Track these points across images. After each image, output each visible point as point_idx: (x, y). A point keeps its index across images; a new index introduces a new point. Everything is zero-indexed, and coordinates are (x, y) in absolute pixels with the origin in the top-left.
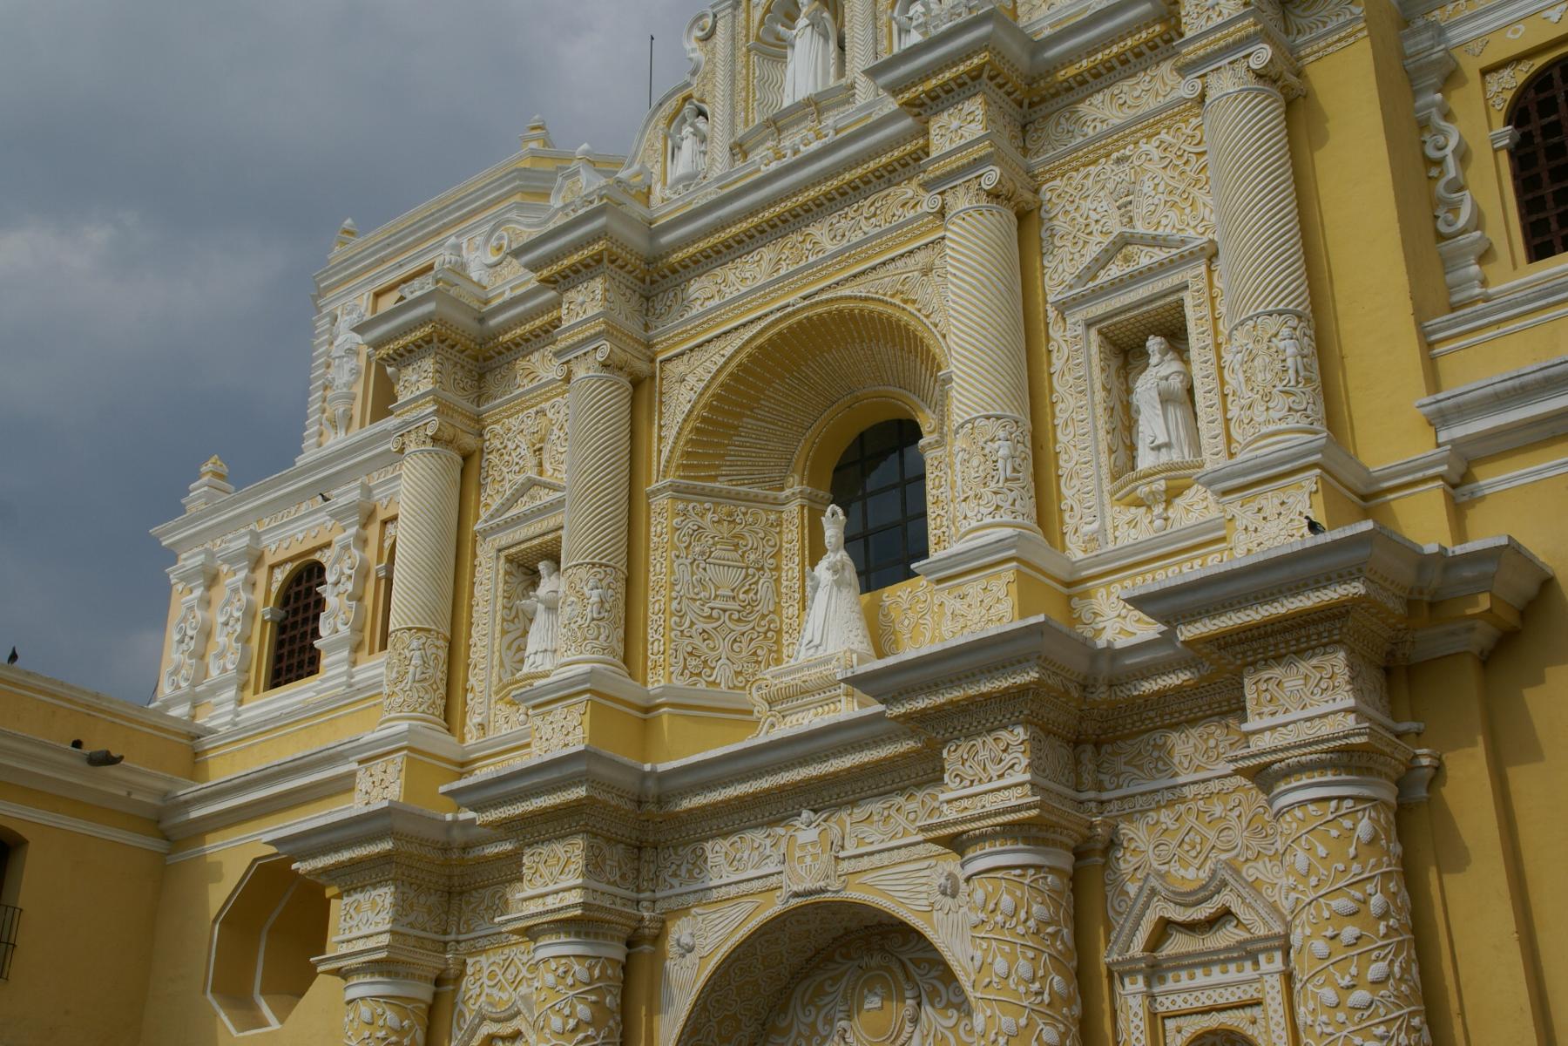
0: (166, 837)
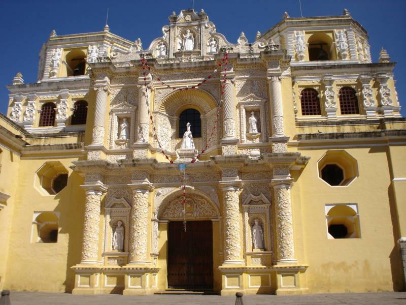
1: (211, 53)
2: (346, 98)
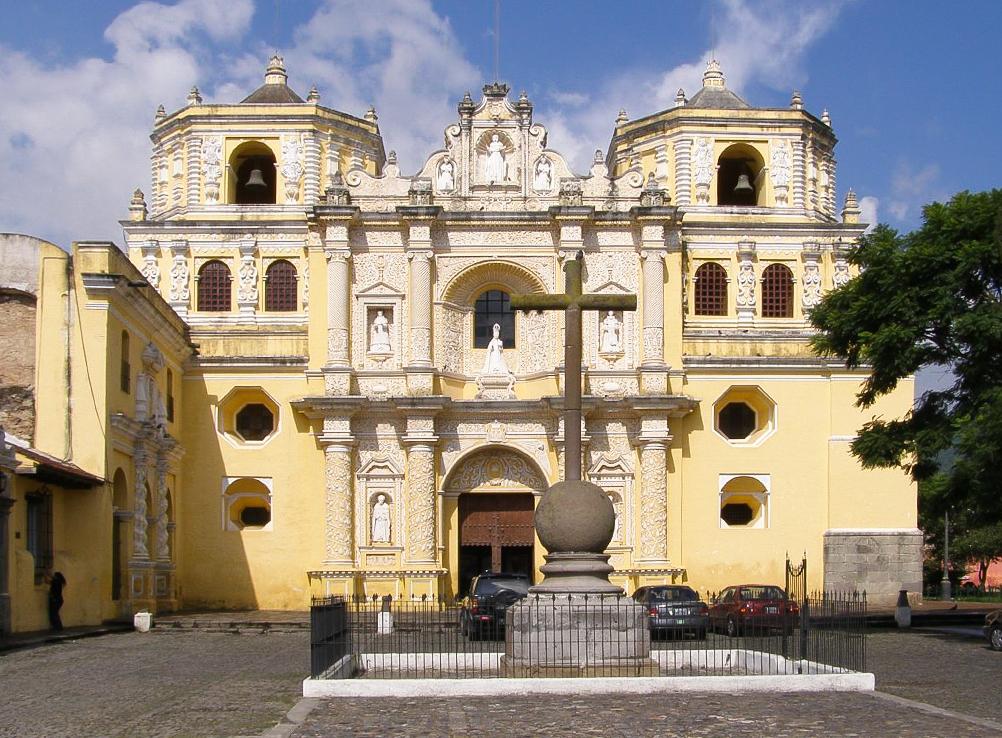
0: (183, 368)
2: (774, 285)
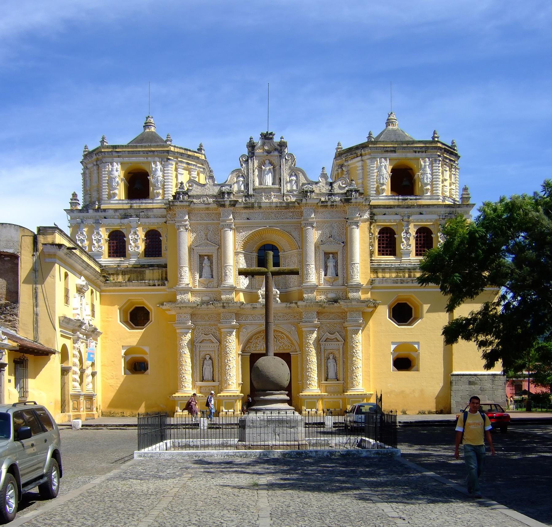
1: (291, 191)
